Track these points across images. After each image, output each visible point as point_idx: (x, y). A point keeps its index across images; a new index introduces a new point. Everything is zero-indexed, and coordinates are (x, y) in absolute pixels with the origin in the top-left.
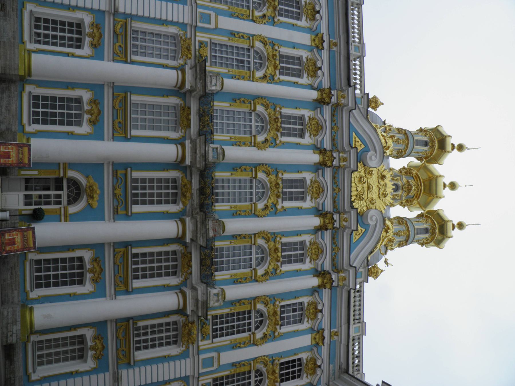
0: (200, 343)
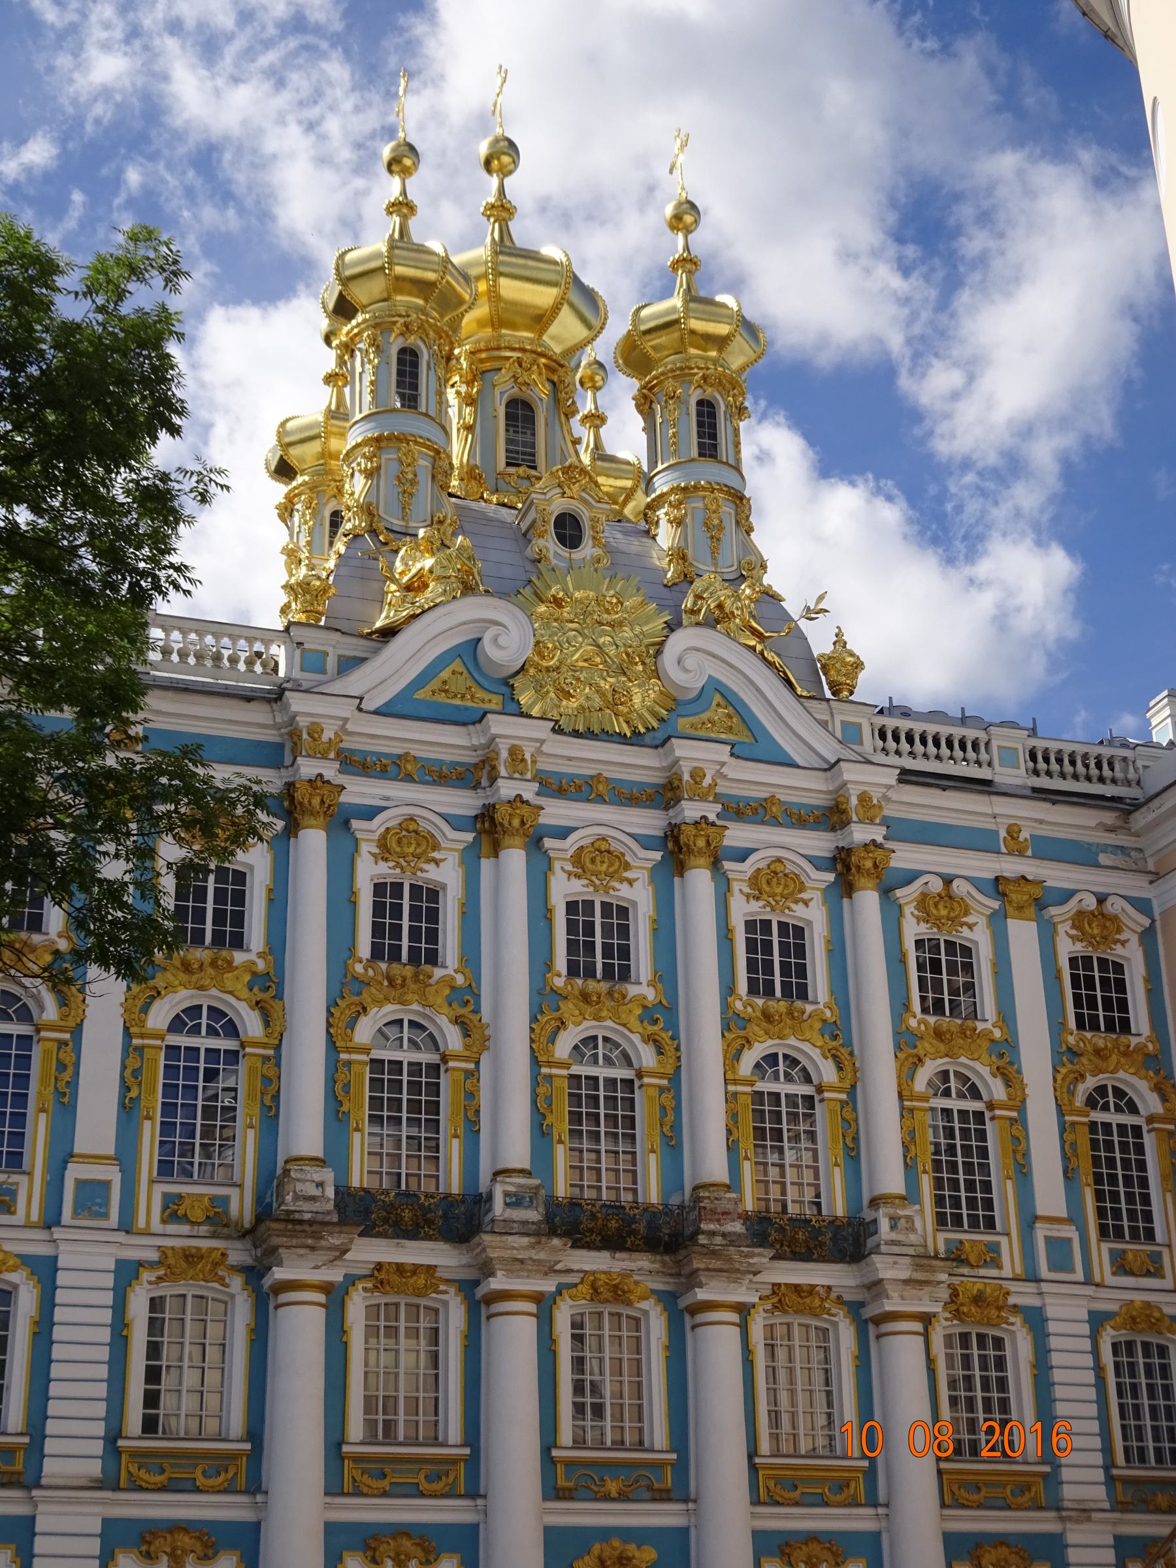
0: (1007, 1272)
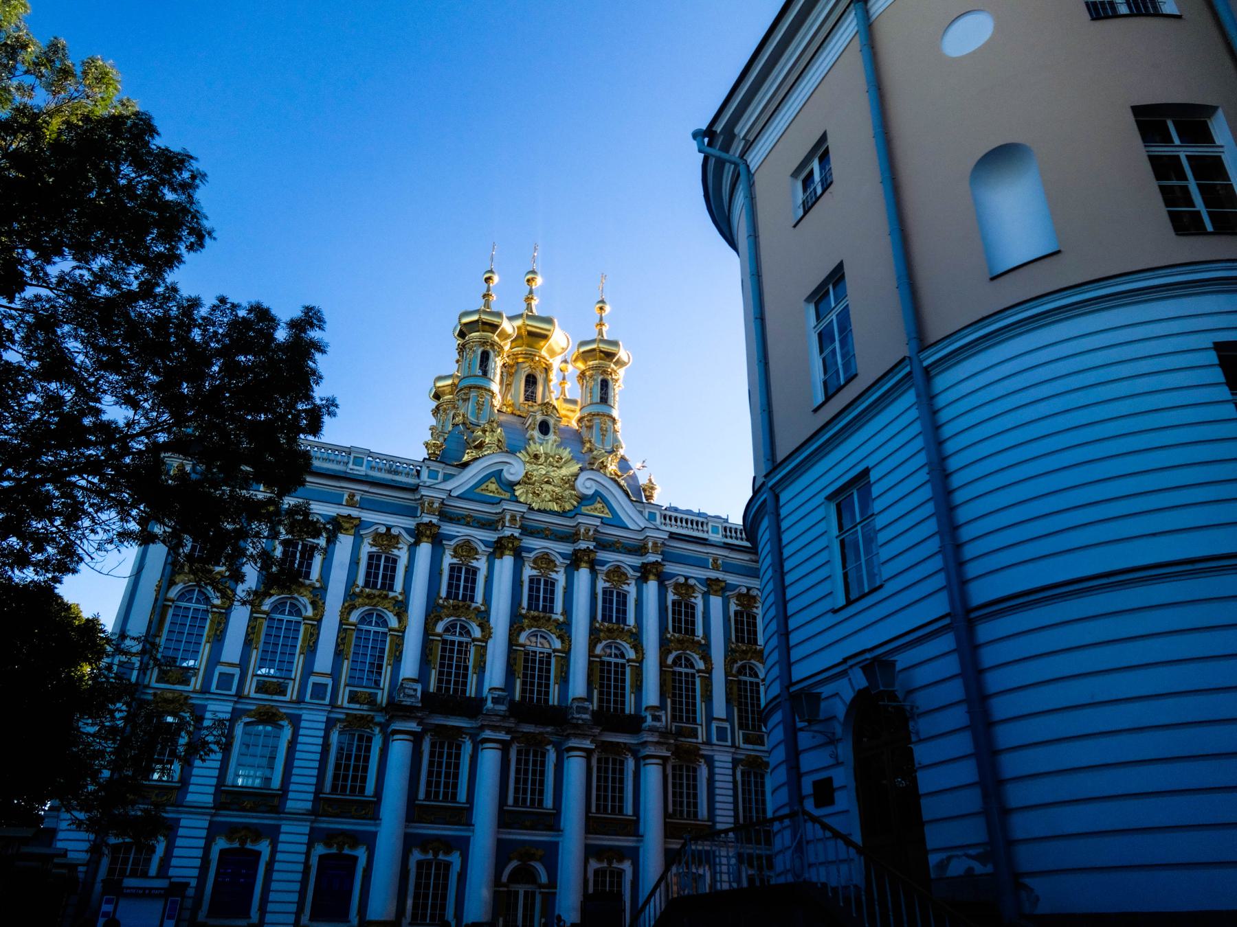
0: (700, 740)
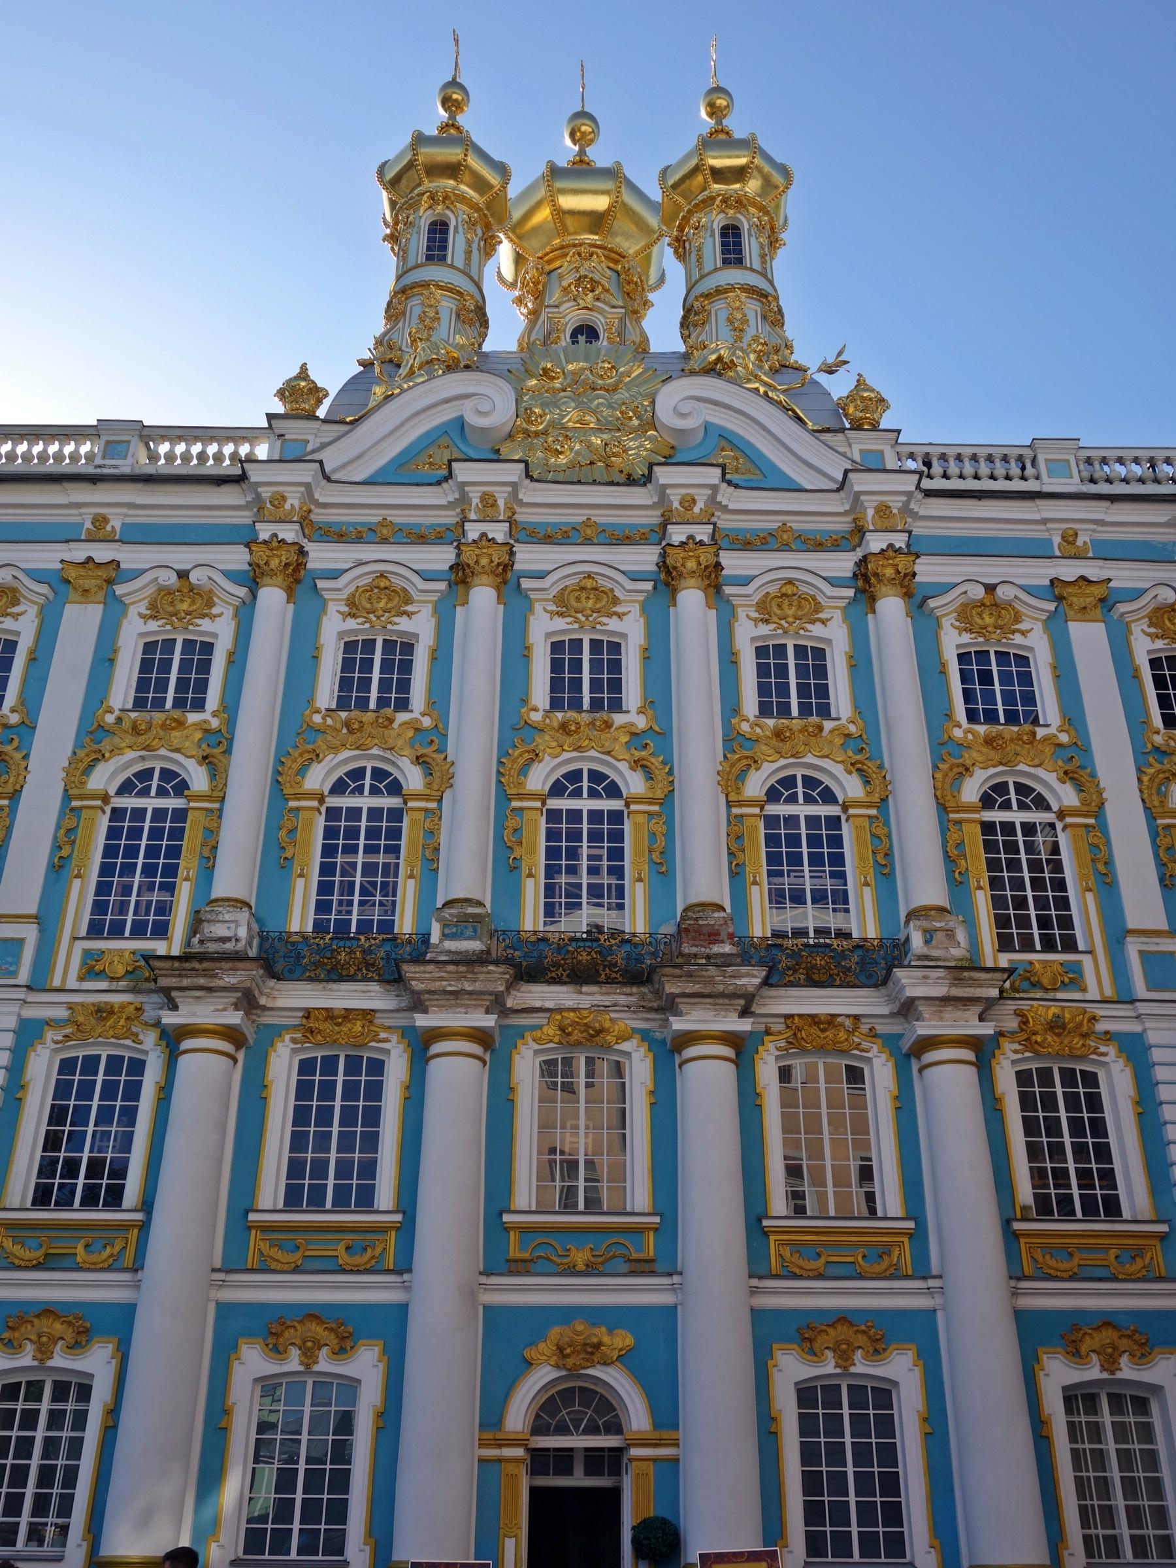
0: (1093, 993)
